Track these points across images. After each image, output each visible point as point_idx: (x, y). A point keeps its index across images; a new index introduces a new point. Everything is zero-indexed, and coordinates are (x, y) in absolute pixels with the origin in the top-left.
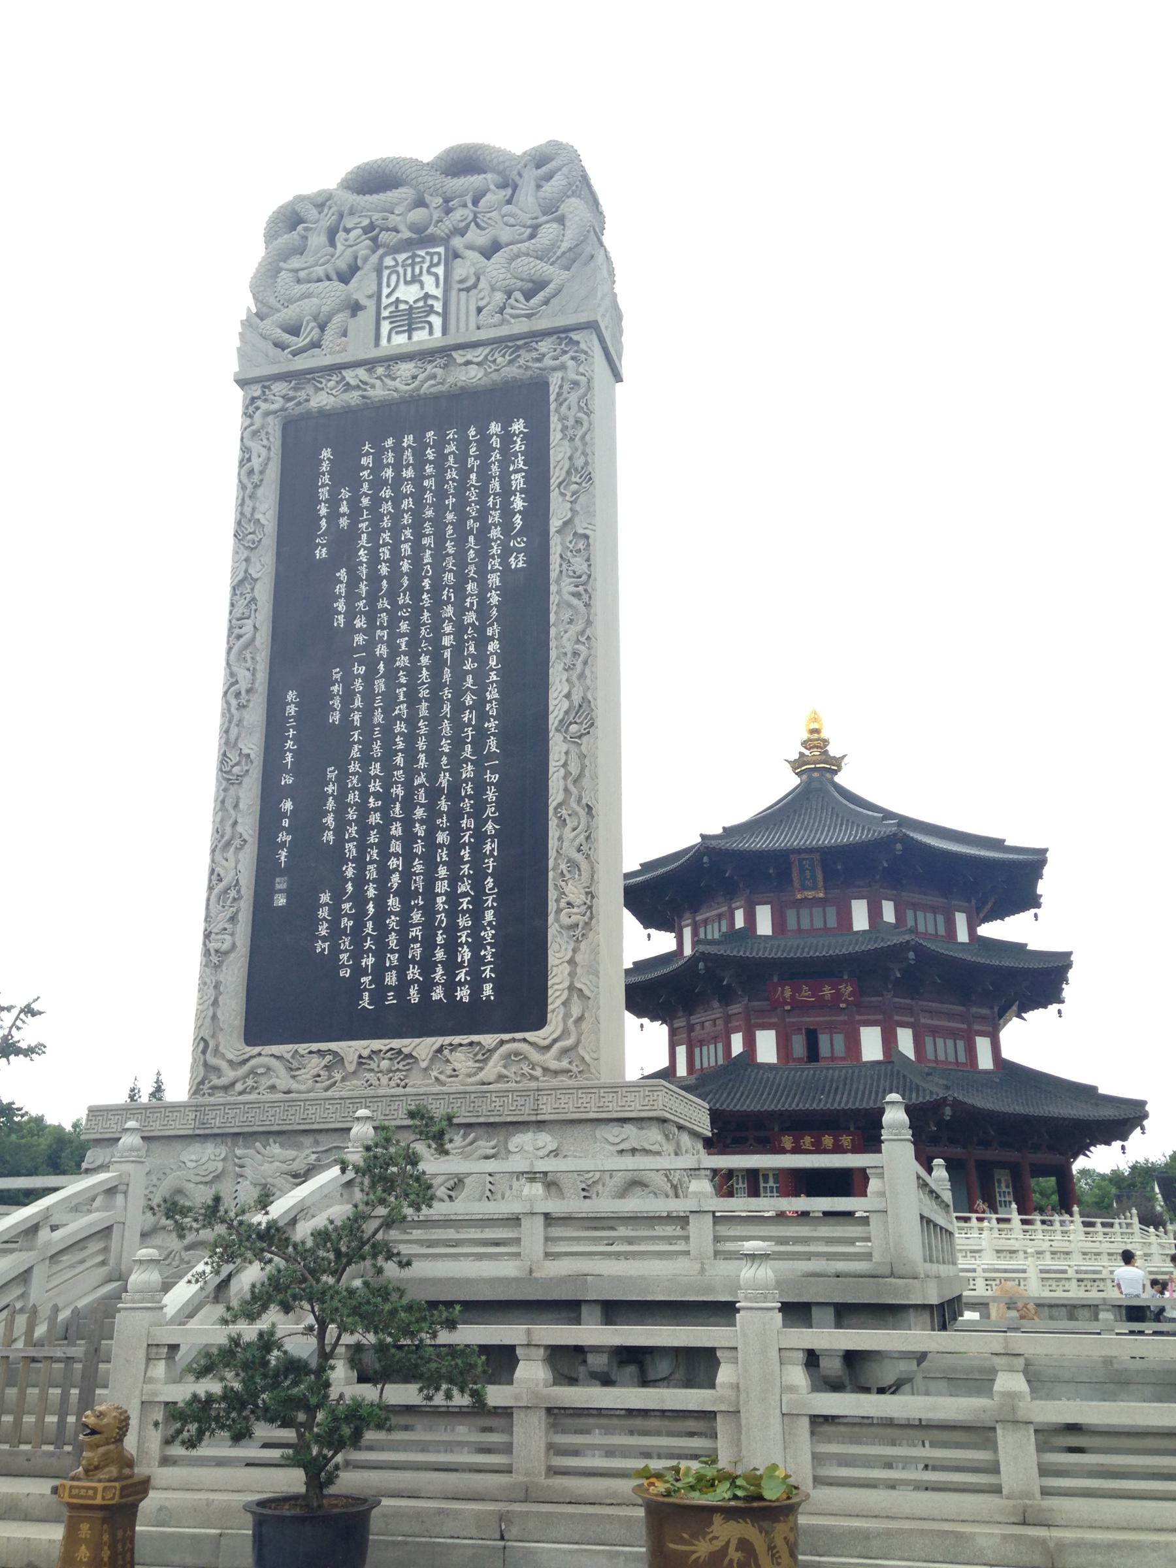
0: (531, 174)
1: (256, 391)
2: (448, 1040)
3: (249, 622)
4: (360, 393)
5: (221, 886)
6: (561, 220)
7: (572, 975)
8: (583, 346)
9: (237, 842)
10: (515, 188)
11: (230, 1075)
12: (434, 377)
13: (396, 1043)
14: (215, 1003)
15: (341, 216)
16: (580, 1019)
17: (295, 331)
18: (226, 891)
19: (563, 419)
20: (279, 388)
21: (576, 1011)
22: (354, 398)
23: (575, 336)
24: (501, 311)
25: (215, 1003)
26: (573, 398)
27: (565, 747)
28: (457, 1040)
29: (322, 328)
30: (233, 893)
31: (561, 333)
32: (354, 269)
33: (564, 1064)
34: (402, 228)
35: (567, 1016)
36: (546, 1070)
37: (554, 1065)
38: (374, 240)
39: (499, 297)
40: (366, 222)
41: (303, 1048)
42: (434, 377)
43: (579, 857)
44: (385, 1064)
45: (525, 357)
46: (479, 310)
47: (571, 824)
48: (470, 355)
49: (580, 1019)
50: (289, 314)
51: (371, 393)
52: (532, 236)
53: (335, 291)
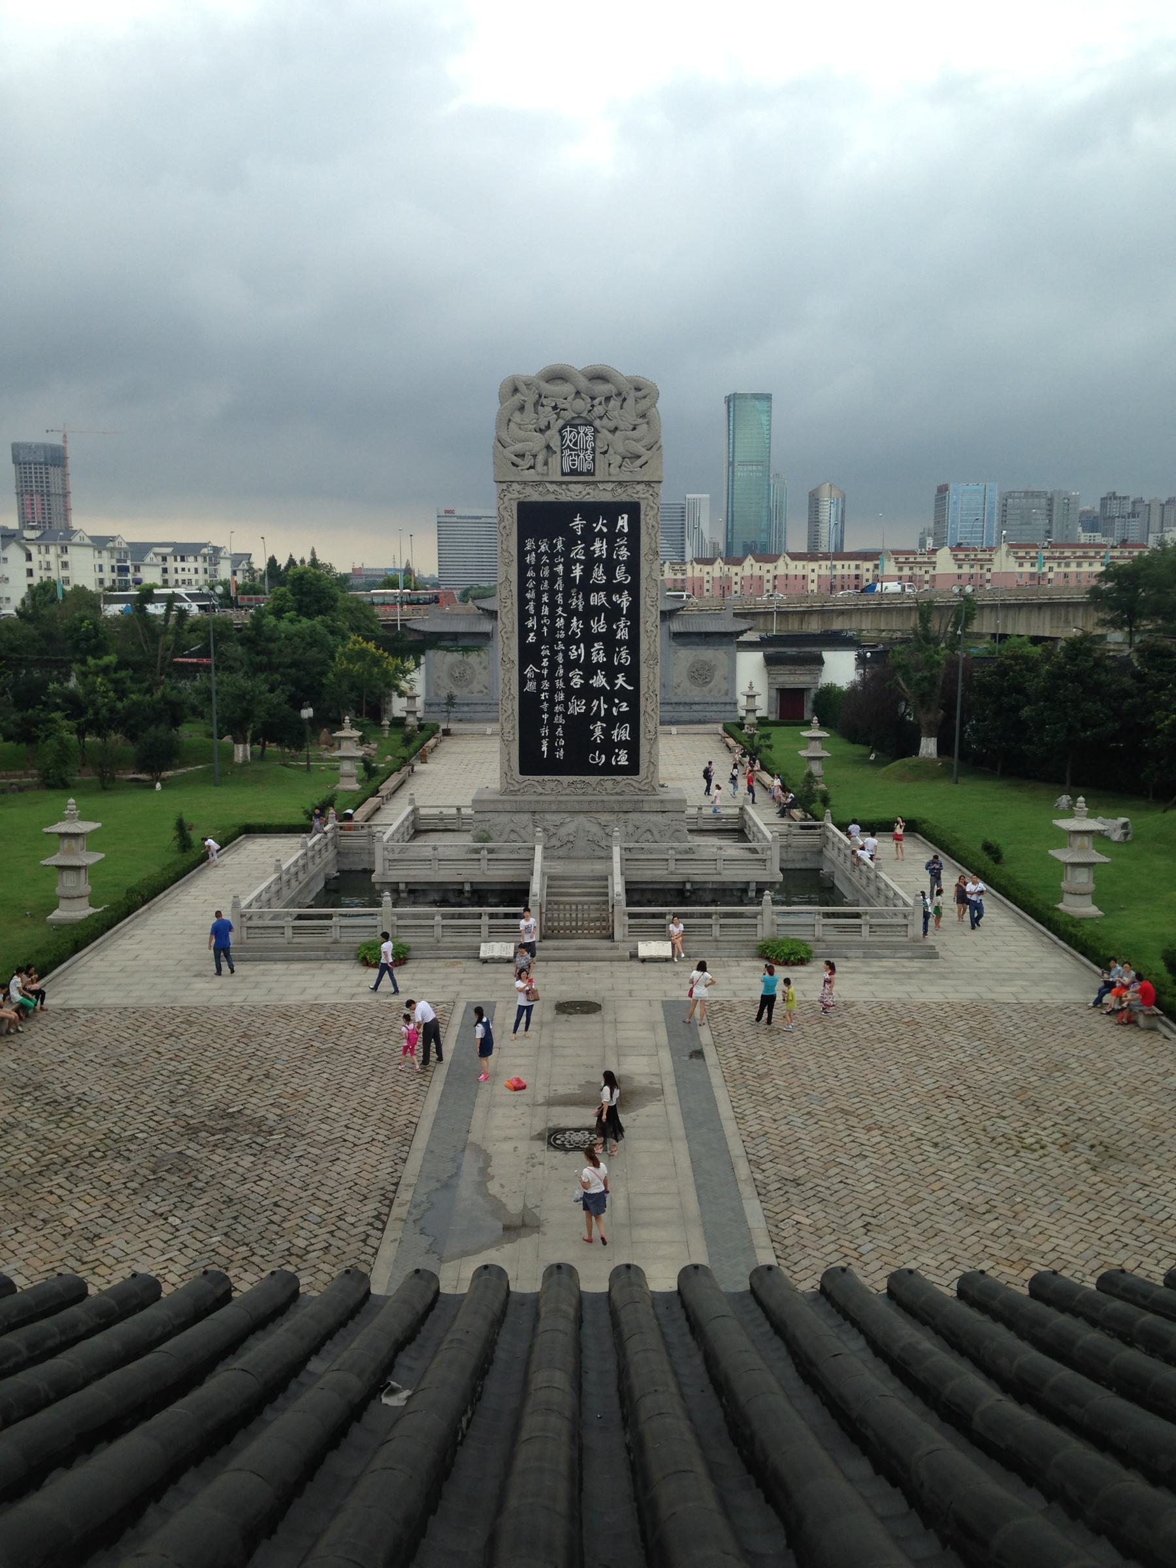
0: (633, 393)
1: (504, 486)
2: (602, 777)
3: (509, 601)
4: (554, 496)
5: (507, 714)
6: (648, 423)
7: (651, 757)
8: (656, 490)
9: (511, 697)
10: (625, 399)
11: (517, 787)
12: (588, 494)
13: (582, 778)
14: (509, 760)
15: (540, 396)
16: (653, 772)
17: (521, 456)
18: (509, 716)
19: (646, 523)
20: (516, 486)
21: (652, 770)
22: (551, 498)
23: (652, 485)
24: (620, 467)
25: (509, 760)
26: (651, 513)
27: (647, 670)
28: (606, 778)
29: (535, 456)
30: (511, 718)
31: (648, 483)
32: (548, 427)
33: (646, 788)
34: (570, 410)
35: (649, 771)
36: (640, 789)
37: (643, 788)
38: (558, 414)
39: (619, 459)
40: (553, 404)
41: (547, 777)
42: (588, 494)
43: (652, 713)
44: (579, 786)
45: (630, 490)
46: (610, 464)
47: (650, 701)
48: (605, 486)
49: (653, 772)
50: (518, 447)
51: (560, 497)
52: (634, 429)
53: (538, 441)
